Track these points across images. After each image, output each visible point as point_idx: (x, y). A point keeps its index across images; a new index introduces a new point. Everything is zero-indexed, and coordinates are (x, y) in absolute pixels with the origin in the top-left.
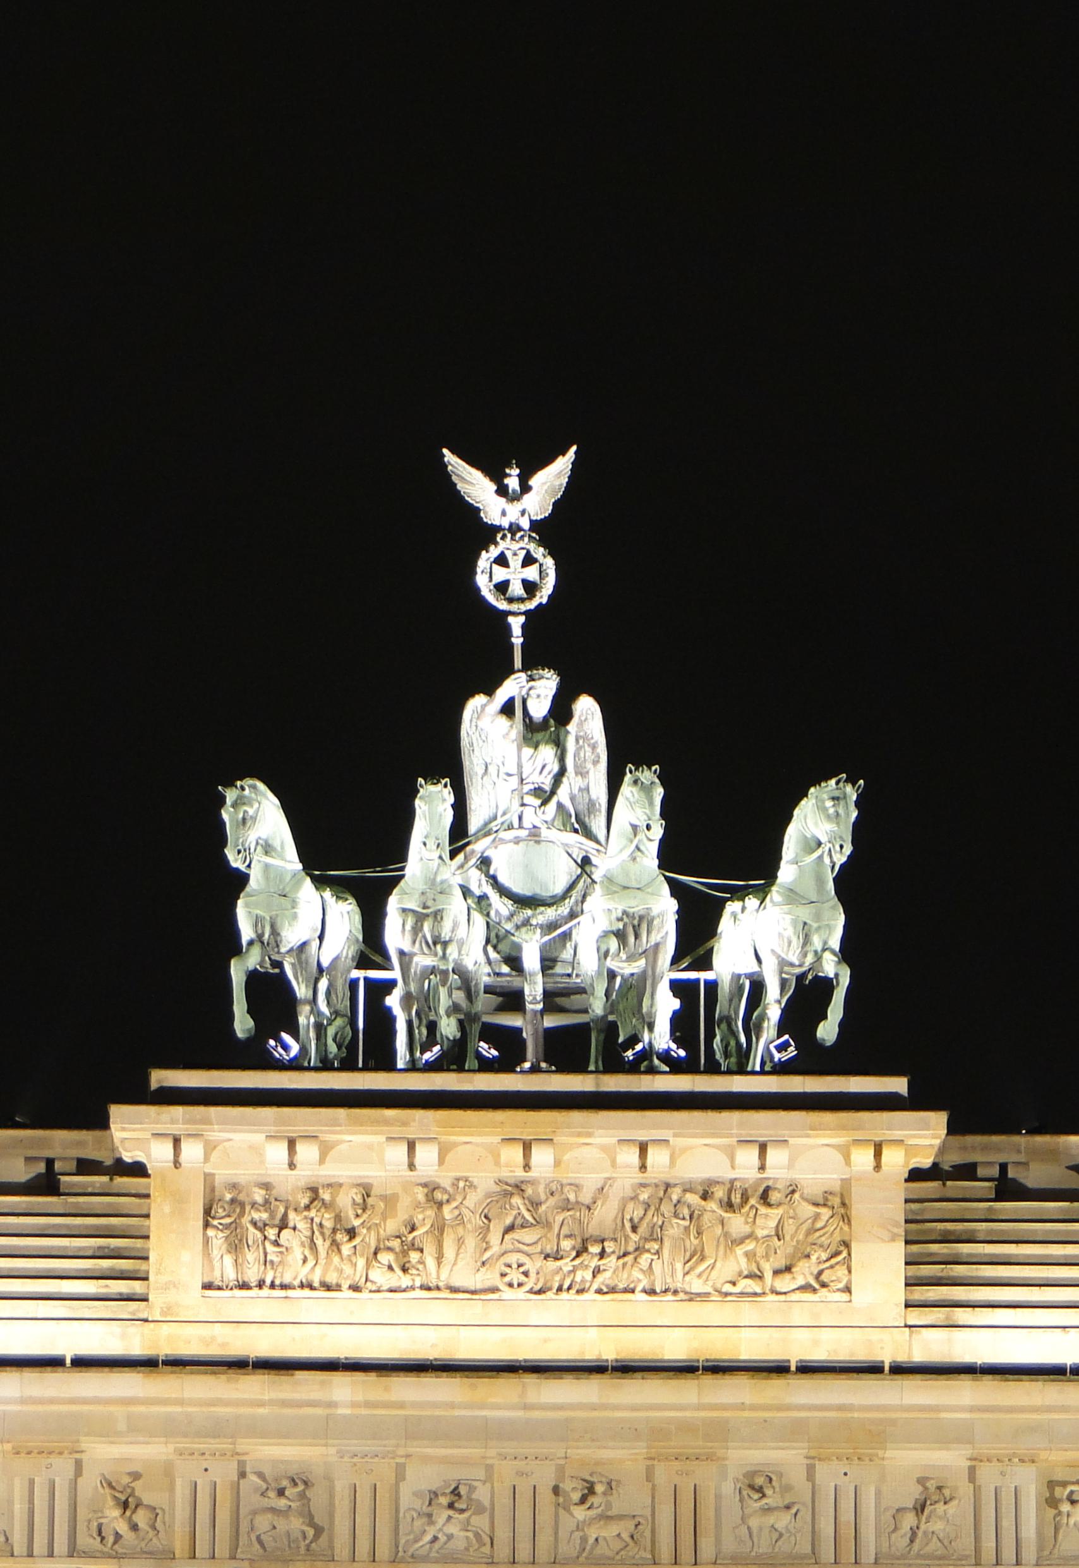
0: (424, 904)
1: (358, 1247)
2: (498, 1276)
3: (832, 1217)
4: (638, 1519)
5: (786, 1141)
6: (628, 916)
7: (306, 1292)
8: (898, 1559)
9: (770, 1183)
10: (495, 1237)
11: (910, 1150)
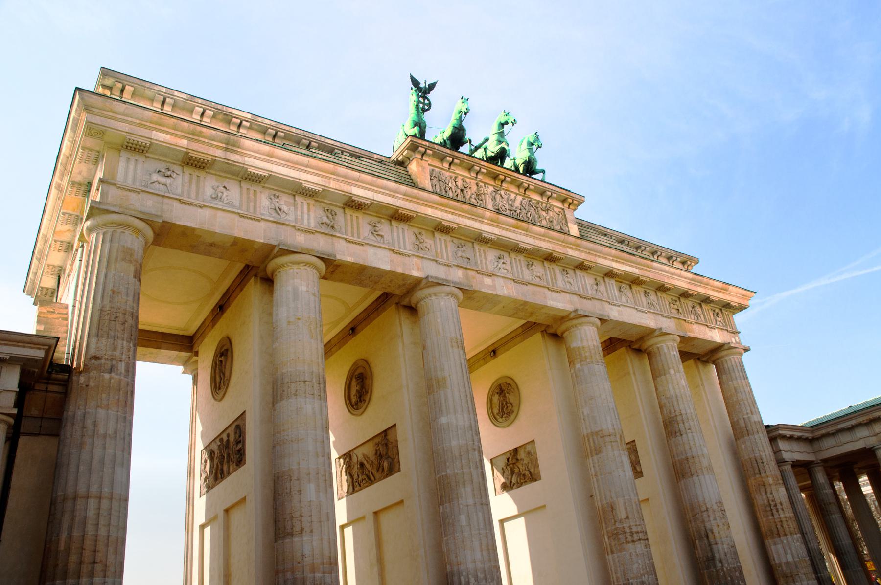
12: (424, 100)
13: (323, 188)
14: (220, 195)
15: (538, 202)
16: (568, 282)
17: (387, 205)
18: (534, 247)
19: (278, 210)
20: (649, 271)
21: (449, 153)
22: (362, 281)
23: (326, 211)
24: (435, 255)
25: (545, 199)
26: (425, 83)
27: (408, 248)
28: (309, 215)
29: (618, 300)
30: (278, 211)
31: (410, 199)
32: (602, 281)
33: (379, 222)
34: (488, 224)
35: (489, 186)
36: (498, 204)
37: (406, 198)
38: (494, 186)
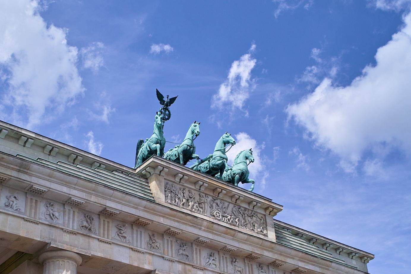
14: (11, 203)
15: (246, 209)
18: (238, 248)
19: (52, 216)
20: (328, 270)
22: (107, 268)
23: (86, 216)
24: (163, 252)
25: (251, 207)
26: (168, 96)
27: (143, 247)
28: (73, 220)
30: (52, 216)
31: (148, 210)
33: (124, 226)
34: (204, 230)
35: (208, 196)
37: (145, 209)
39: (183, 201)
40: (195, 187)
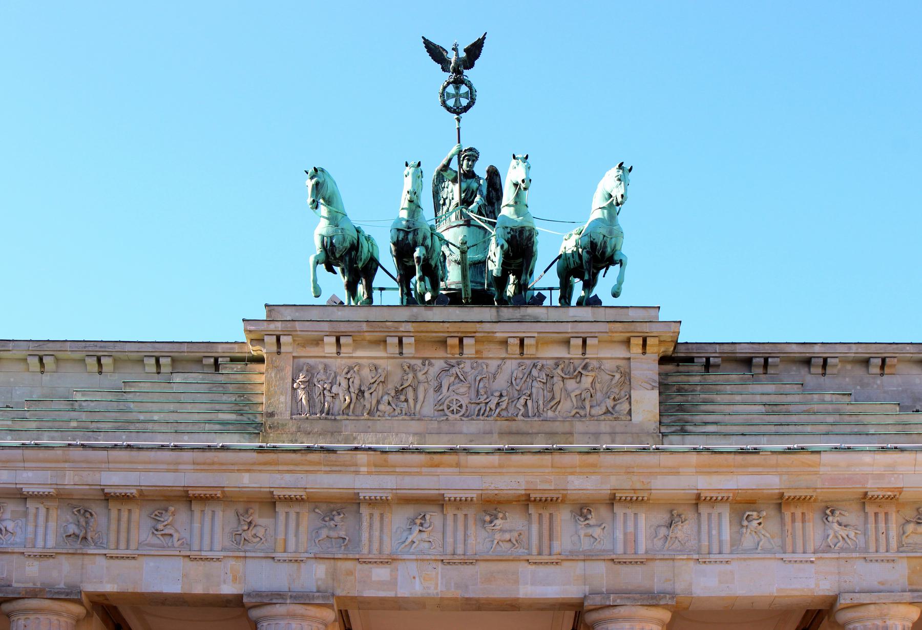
0: (408, 226)
1: (373, 394)
2: (445, 409)
3: (621, 377)
4: (521, 532)
5: (596, 337)
6: (513, 231)
7: (345, 417)
8: (658, 551)
9: (588, 360)
10: (444, 389)
11: (661, 342)
12: (457, 88)
13: (55, 487)
15: (558, 362)
16: (586, 535)
17: (161, 488)
21: (327, 330)
23: (76, 513)
25: (576, 352)
27: (217, 546)
28: (46, 528)
29: (727, 548)
32: (690, 515)
34: (370, 473)
35: (433, 361)
36: (443, 400)
37: (198, 467)
38: (447, 358)
39: (345, 400)
40: (387, 353)
